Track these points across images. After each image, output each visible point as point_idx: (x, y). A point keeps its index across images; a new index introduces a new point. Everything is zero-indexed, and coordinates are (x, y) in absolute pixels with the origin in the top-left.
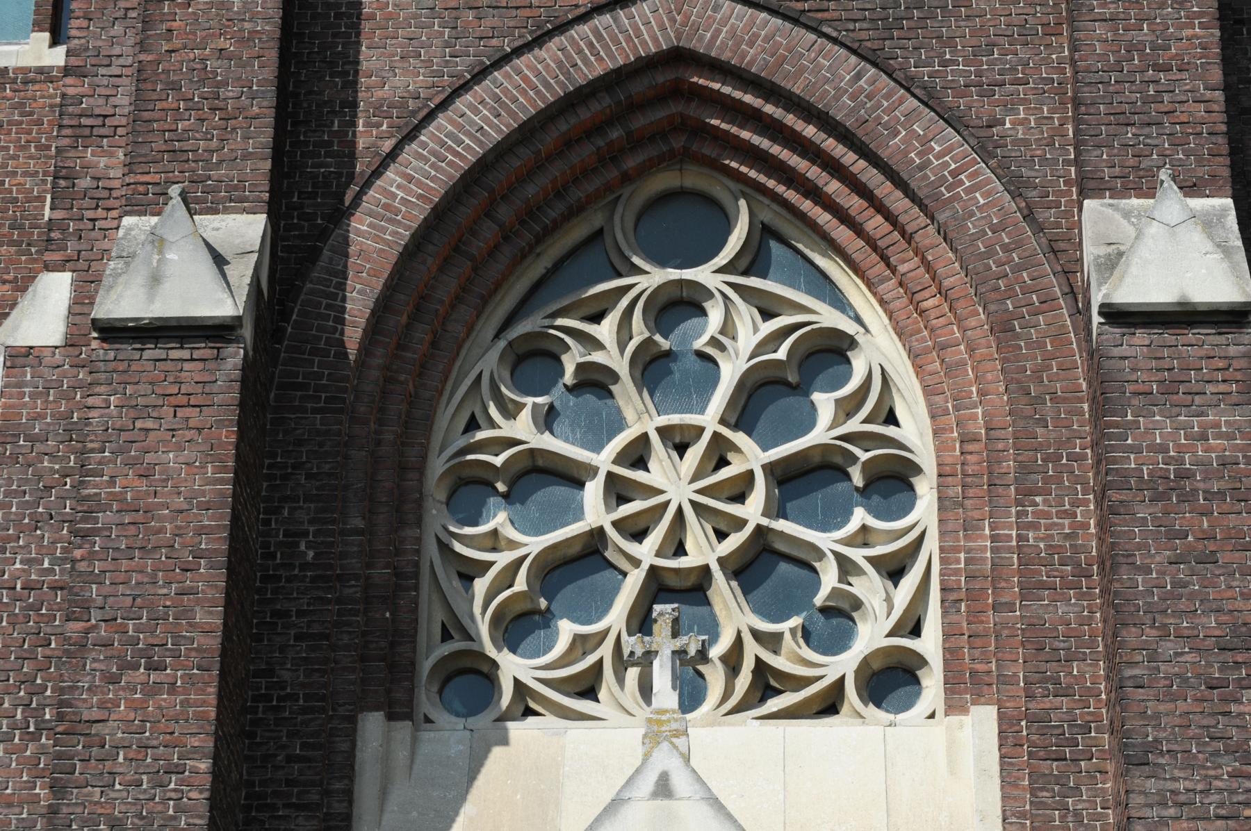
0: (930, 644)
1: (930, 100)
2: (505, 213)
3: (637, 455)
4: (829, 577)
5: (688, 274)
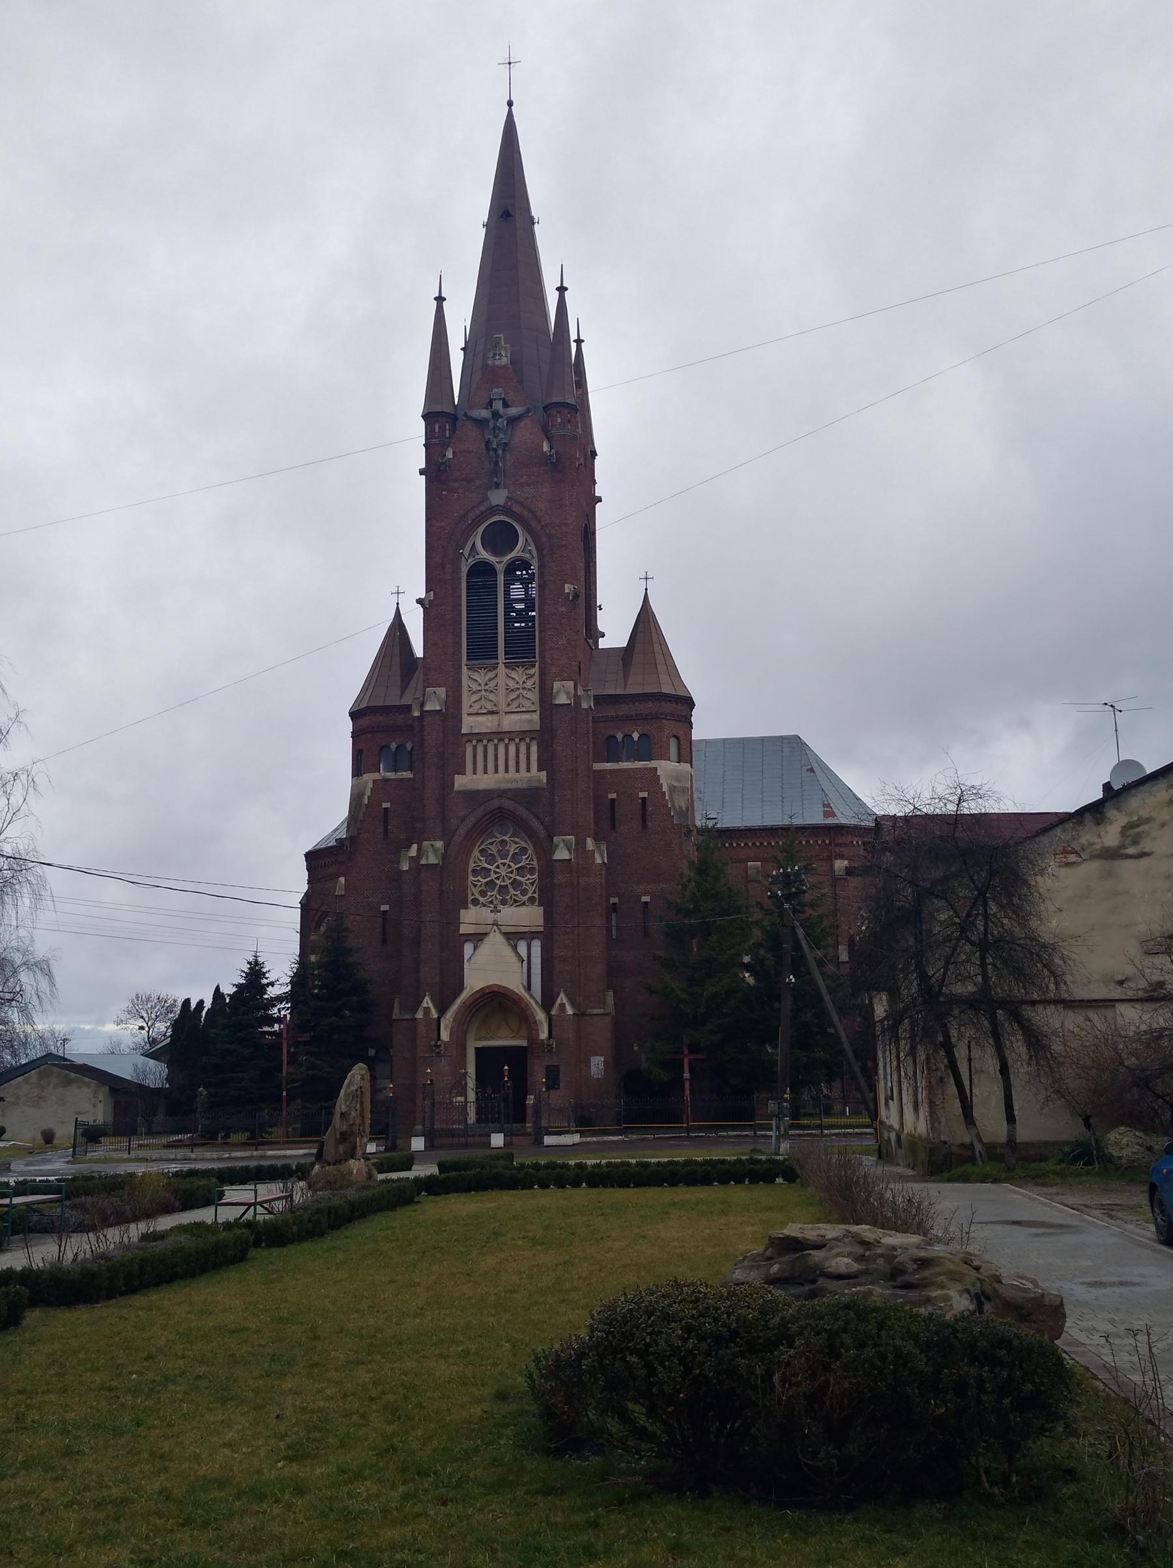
0: (536, 895)
1: (535, 815)
2: (478, 831)
3: (498, 867)
4: (524, 886)
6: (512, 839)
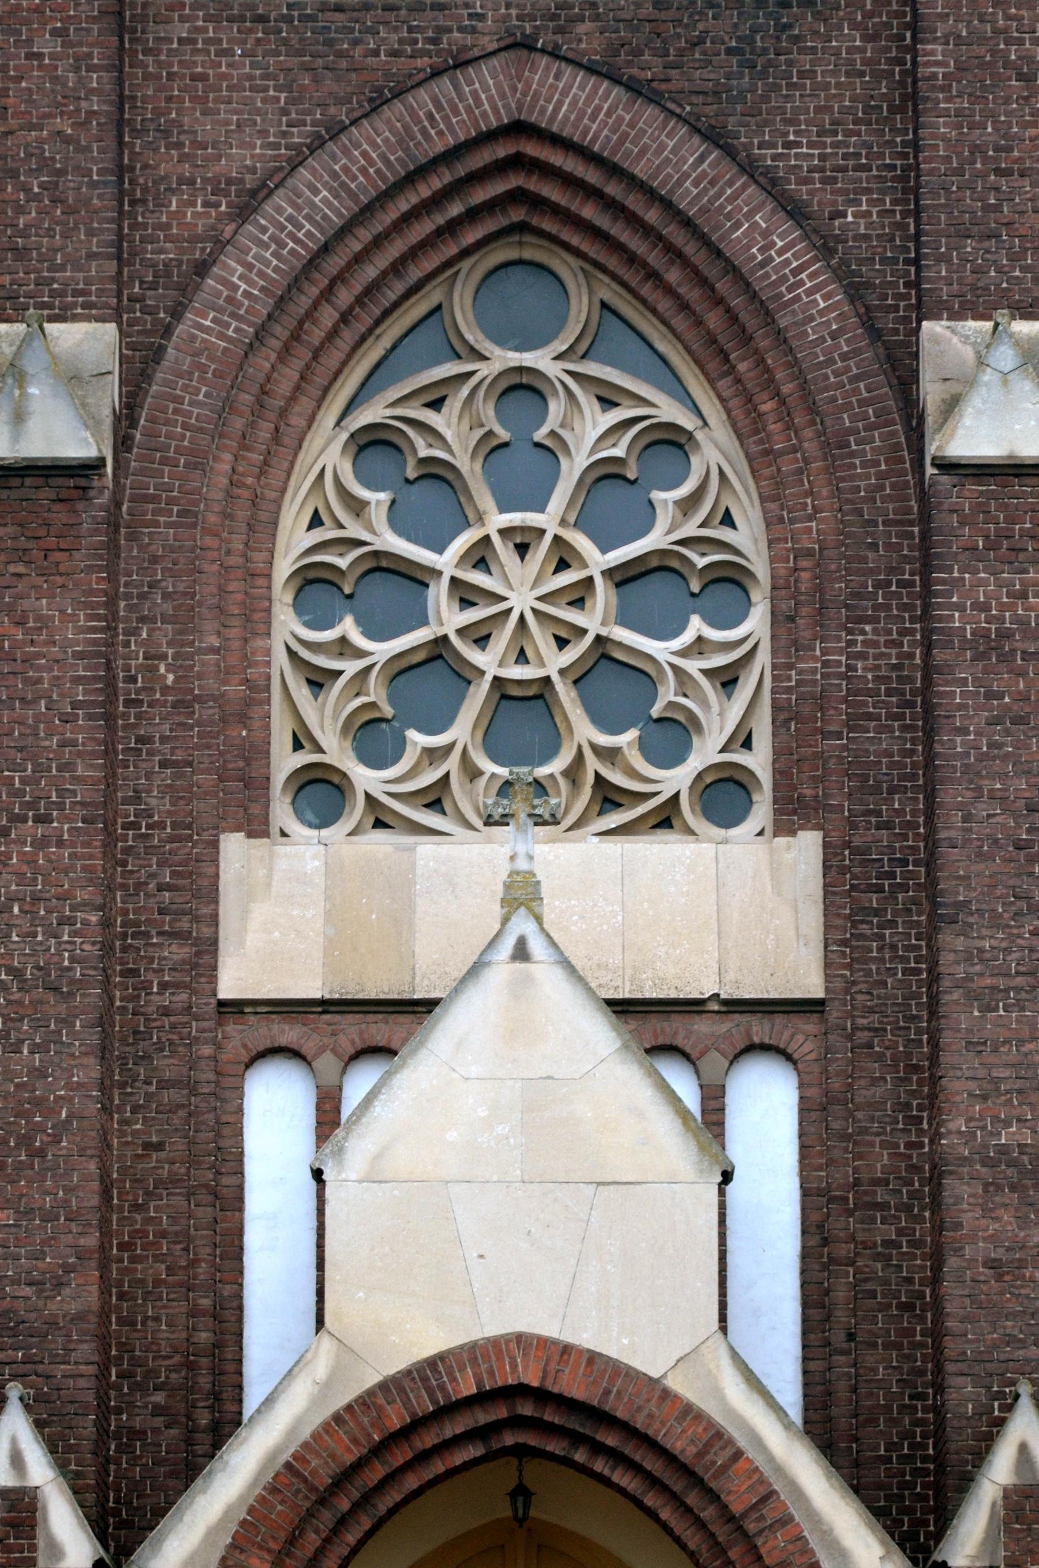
2: (345, 297)
4: (668, 693)
5: (528, 359)
6: (592, 368)
